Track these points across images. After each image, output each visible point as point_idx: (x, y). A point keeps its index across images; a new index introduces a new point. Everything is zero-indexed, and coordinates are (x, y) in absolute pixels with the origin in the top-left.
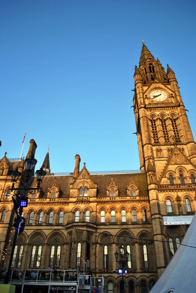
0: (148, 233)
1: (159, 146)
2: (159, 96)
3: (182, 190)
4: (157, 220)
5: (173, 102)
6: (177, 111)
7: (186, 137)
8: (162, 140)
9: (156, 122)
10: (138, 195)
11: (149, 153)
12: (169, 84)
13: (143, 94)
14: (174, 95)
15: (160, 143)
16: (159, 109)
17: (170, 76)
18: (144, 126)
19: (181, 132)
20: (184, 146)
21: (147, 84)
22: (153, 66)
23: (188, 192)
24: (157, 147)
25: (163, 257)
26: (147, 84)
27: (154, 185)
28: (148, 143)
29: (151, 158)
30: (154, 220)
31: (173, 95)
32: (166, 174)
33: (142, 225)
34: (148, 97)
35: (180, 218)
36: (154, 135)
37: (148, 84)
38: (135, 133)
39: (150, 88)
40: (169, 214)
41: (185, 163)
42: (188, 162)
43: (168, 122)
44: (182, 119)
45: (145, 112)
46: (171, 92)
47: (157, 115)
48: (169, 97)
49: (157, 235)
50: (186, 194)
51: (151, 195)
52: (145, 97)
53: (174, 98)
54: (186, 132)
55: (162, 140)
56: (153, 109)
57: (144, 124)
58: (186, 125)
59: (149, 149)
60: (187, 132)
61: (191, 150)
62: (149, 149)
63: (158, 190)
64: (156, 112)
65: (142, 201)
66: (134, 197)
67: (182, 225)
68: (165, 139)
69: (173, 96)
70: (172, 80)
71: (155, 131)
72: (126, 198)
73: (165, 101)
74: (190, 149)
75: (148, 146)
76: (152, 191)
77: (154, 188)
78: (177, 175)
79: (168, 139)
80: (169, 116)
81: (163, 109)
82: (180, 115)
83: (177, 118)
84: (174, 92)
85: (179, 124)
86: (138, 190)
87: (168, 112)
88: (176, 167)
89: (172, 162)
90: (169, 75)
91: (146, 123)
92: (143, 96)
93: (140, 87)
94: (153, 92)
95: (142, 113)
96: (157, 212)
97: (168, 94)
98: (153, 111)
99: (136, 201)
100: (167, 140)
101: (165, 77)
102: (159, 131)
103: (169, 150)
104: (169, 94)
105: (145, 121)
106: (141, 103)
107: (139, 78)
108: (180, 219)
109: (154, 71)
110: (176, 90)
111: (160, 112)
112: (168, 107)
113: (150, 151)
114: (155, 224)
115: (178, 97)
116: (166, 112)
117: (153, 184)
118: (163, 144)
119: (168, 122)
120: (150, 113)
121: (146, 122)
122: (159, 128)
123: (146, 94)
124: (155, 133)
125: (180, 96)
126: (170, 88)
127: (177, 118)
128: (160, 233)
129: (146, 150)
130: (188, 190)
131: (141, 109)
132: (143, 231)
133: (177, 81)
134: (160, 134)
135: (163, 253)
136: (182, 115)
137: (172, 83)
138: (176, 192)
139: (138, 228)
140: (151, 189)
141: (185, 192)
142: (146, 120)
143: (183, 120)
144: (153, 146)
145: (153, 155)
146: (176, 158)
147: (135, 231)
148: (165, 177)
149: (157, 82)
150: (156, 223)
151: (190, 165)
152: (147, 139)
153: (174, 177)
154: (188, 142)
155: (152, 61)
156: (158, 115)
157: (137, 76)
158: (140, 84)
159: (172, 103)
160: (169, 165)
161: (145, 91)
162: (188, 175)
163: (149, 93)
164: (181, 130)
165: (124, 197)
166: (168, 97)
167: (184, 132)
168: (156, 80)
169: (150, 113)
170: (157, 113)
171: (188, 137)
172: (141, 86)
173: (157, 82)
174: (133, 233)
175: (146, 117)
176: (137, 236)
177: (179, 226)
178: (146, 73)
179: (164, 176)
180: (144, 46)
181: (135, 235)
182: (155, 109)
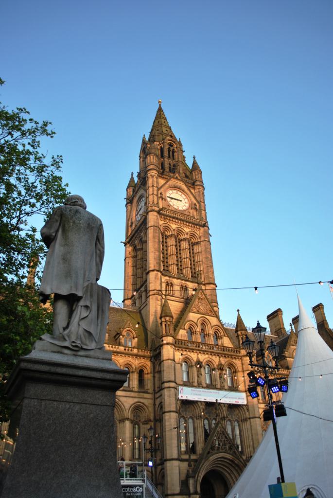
0: (145, 407)
1: (170, 277)
2: (178, 200)
3: (203, 352)
4: (173, 390)
5: (196, 218)
6: (200, 232)
7: (206, 274)
8: (174, 269)
9: (168, 240)
10: (136, 346)
11: (158, 285)
12: (193, 188)
13: (159, 189)
14: (198, 207)
15: (170, 273)
16: (177, 221)
17: (197, 177)
18: (154, 241)
19: (200, 265)
21: (164, 176)
22: (173, 149)
23: (211, 356)
24: (168, 278)
25: (176, 445)
26: (164, 176)
27: (171, 338)
28: (157, 268)
29: (159, 293)
30: (168, 389)
31: (196, 205)
32: (185, 324)
33: (137, 394)
34: (163, 196)
35: (199, 391)
36: (163, 257)
37: (166, 177)
38: (124, 243)
39: (168, 184)
40: (185, 384)
41: (210, 314)
42: (213, 313)
43: (184, 245)
44: (205, 246)
45: (157, 219)
46: (195, 202)
47: (172, 229)
48: (192, 208)
49: (170, 412)
50: (208, 359)
51: (166, 353)
52: (159, 195)
53: (197, 211)
54: (208, 266)
55: (174, 269)
56: (168, 218)
57: (154, 237)
58: (208, 257)
59: (158, 279)
60: (209, 268)
61: (211, 295)
62: (158, 279)
63: (175, 347)
64: (171, 225)
65: (140, 356)
66: (130, 349)
67: (200, 402)
68: (178, 269)
69: (196, 208)
71: (165, 252)
72: (118, 348)
73: (185, 210)
74: (210, 294)
75: (157, 274)
76: (169, 347)
77: (171, 342)
78: (198, 329)
79: (181, 270)
80: (188, 237)
81: (182, 222)
82: (202, 239)
83: (198, 243)
84: (198, 203)
85: (199, 252)
86: (136, 339)
87: (187, 230)
88: (199, 317)
89: (194, 308)
90: (195, 175)
91: (157, 238)
92: (158, 193)
93: (154, 177)
94: (170, 192)
95: (154, 219)
96: (173, 380)
97: (190, 202)
98: (168, 221)
99: (133, 355)
100: (180, 271)
101: (187, 174)
102: (171, 255)
103: (182, 287)
104: (192, 202)
105: (156, 233)
106: (153, 203)
107: (155, 162)
108: (198, 393)
109: (173, 159)
110: (202, 200)
111: (177, 226)
112: (189, 222)
113: (159, 282)
114: (169, 396)
115: (203, 212)
116: (185, 229)
117: (171, 336)
118: (175, 276)
119: (184, 245)
120: (163, 222)
121: (157, 235)
122: (172, 250)
123: (161, 190)
124: (166, 257)
125: (205, 210)
126: (194, 193)
127: (198, 243)
128: (175, 410)
129: (154, 279)
130: (211, 353)
131: (152, 213)
132: (138, 402)
133: (204, 186)
134: (172, 260)
135: (176, 439)
136: (205, 241)
137: (198, 187)
138: (196, 354)
139: (132, 397)
140: (167, 344)
141: (207, 356)
142: (158, 232)
143: (206, 248)
144: (163, 275)
146: (200, 304)
147: (126, 402)
148: (184, 329)
149: (179, 178)
150: (170, 394)
151: (215, 318)
152: (157, 263)
153: (194, 330)
154: (208, 282)
155: (174, 142)
156: (174, 230)
157: (152, 157)
158: (156, 172)
159: (194, 217)
160: (190, 312)
161: (160, 185)
162: (211, 332)
163: (165, 191)
164: (201, 262)
165: (112, 345)
166: (190, 207)
167: (205, 266)
168: (177, 175)
169: (163, 222)
170: (174, 226)
171: (209, 275)
172: (156, 175)
173: (179, 178)
174: (124, 404)
176: (130, 409)
177: (197, 402)
178: (162, 156)
179: (183, 328)
180: (160, 110)
181: (126, 408)
182: (171, 219)
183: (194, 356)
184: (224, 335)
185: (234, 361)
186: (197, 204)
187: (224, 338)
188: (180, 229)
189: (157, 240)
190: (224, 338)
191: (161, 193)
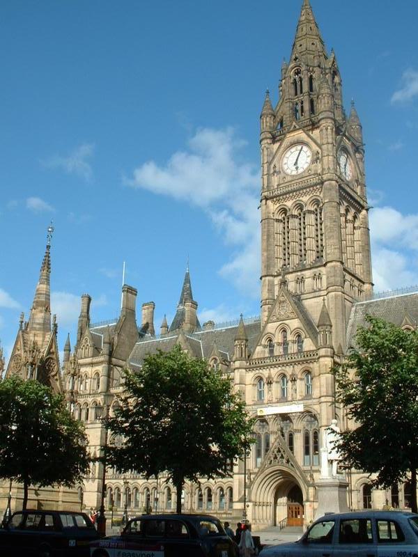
20: (323, 270)
23: (284, 368)
26: (278, 138)
28: (265, 274)
46: (315, 148)
62: (265, 286)
63: (245, 369)
69: (318, 158)
70: (320, 117)
87: (305, 199)
92: (268, 170)
107: (265, 126)
111: (294, 200)
121: (266, 230)
130: (283, 364)
144: (275, 276)
145: (271, 297)
148: (261, 345)
152: (265, 267)
163: (281, 159)
169: (278, 205)
175: (268, 218)
183: (265, 373)
184: (306, 337)
185: (311, 365)
186: (320, 151)
187: (305, 340)
188: (298, 202)
189: (265, 237)
190: (305, 340)
191: (275, 167)
